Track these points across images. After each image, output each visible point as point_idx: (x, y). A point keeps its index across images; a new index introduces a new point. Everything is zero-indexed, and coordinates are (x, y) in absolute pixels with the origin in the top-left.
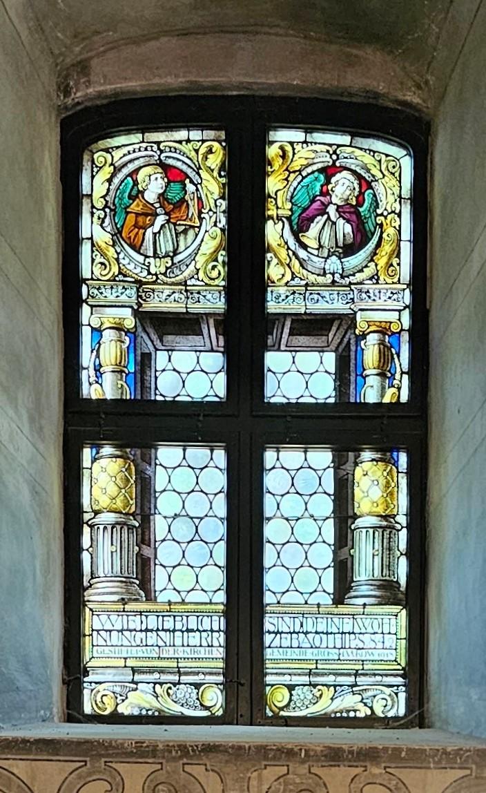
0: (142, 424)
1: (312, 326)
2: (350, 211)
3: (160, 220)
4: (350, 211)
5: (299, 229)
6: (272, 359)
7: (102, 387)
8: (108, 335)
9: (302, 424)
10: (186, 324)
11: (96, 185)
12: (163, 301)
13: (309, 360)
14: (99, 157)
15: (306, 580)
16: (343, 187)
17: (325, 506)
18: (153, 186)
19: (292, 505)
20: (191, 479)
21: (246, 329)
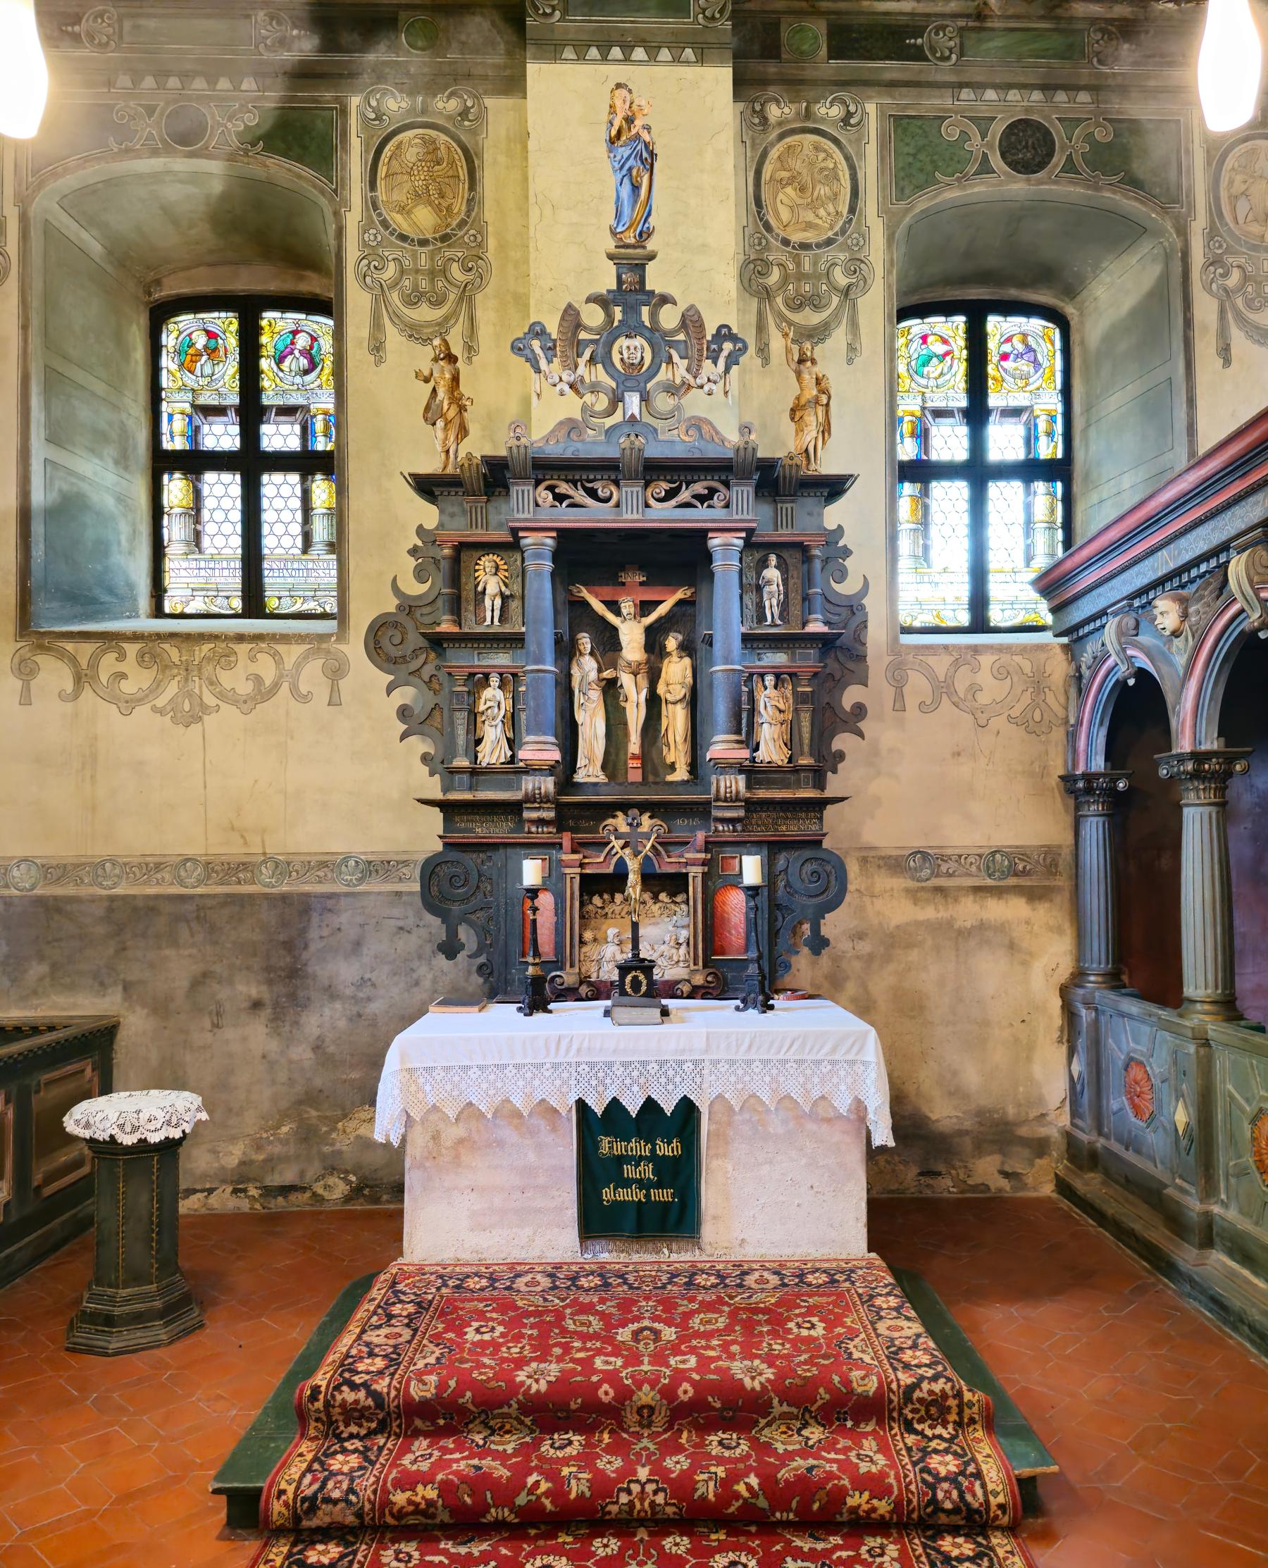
0: (195, 462)
1: (287, 411)
2: (307, 353)
3: (205, 358)
4: (307, 353)
5: (280, 360)
6: (265, 429)
7: (174, 442)
8: (177, 417)
9: (282, 462)
10: (219, 411)
11: (169, 340)
12: (207, 399)
13: (285, 429)
14: (171, 327)
15: (287, 542)
16: (302, 341)
17: (296, 503)
18: (201, 341)
19: (279, 503)
20: (223, 489)
21: (251, 412)
